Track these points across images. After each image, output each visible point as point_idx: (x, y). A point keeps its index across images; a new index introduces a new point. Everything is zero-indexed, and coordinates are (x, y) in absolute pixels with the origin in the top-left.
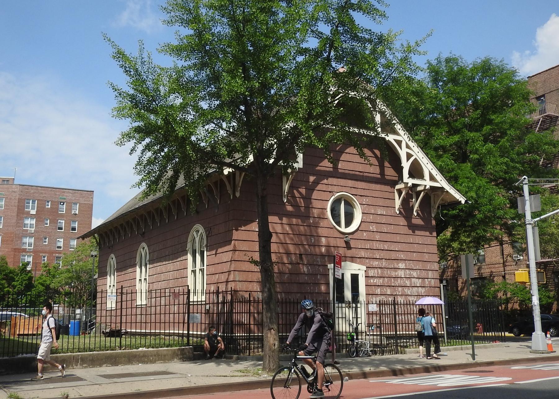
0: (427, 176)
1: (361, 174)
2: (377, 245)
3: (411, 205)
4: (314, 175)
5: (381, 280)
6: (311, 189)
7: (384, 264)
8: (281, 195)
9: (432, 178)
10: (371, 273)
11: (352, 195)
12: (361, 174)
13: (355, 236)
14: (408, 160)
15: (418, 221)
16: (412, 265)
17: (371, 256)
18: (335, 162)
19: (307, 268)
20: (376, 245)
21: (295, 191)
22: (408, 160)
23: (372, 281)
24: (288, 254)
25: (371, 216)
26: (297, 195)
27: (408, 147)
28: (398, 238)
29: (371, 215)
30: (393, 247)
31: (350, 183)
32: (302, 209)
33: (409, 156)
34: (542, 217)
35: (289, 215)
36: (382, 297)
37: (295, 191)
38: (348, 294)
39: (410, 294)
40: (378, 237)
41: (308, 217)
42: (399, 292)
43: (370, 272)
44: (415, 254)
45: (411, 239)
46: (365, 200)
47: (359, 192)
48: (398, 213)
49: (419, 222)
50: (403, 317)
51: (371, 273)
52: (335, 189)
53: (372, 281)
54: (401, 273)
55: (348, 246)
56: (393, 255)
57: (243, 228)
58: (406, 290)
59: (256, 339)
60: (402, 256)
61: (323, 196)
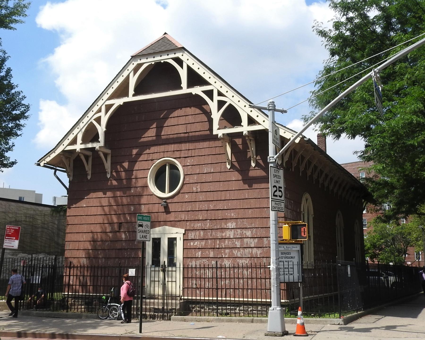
1: (187, 135)
3: (248, 157)
4: (136, 147)
5: (203, 243)
6: (133, 162)
7: (208, 225)
9: (251, 121)
10: (191, 235)
11: (175, 158)
12: (187, 135)
13: (175, 199)
14: (219, 109)
16: (246, 224)
17: (193, 218)
18: (160, 128)
19: (125, 235)
22: (219, 109)
23: (192, 244)
24: (111, 224)
25: (195, 177)
27: (220, 94)
28: (228, 195)
29: (196, 176)
30: (220, 205)
31: (172, 147)
32: (124, 181)
33: (221, 104)
35: (113, 189)
36: (204, 260)
37: (118, 167)
38: (164, 259)
39: (239, 255)
40: (202, 197)
41: (129, 188)
42: (225, 254)
43: (190, 235)
44: (250, 211)
46: (189, 161)
48: (229, 167)
51: (191, 235)
52: (155, 156)
54: (230, 234)
55: (167, 210)
57: (74, 206)
59: (80, 297)
60: (233, 215)
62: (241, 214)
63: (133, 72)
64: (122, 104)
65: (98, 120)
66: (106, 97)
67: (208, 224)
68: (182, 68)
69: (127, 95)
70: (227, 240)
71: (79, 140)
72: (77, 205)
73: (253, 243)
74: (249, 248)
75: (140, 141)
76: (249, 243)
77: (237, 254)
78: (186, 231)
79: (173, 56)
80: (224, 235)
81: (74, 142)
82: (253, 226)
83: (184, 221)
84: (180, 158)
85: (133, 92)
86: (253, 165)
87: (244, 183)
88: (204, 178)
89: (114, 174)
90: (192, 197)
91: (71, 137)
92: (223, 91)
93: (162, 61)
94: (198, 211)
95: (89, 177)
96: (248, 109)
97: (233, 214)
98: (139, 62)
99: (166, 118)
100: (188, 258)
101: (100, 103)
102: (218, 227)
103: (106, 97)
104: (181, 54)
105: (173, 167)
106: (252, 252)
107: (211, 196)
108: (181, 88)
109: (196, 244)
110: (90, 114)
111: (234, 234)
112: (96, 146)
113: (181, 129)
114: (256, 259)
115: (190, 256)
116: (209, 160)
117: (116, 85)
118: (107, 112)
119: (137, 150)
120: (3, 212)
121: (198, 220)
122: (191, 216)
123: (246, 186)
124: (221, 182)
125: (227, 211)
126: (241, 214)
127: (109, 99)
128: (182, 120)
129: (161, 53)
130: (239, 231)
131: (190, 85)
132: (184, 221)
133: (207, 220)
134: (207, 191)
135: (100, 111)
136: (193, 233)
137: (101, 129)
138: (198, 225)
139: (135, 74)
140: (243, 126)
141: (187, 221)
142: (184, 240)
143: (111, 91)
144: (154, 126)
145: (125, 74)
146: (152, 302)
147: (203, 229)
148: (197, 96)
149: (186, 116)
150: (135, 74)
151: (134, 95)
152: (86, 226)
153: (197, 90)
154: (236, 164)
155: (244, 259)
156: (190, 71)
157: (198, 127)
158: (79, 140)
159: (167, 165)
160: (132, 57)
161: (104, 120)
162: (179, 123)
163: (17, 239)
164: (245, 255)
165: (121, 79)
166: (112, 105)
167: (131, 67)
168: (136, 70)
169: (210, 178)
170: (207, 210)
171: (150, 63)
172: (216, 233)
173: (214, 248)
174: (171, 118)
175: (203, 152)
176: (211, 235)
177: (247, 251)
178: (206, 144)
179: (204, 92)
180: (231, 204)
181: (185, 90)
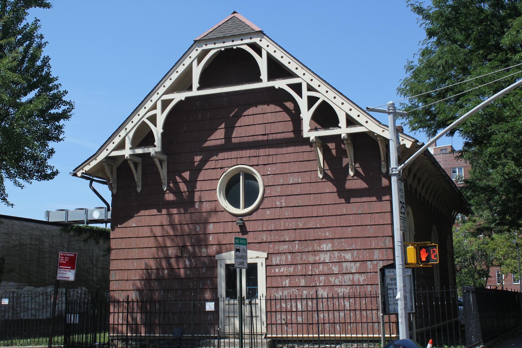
0: (343, 121)
2: (287, 224)
3: (344, 164)
5: (291, 269)
6: (196, 171)
7: (297, 247)
8: (161, 184)
9: (351, 122)
10: (276, 260)
12: (265, 138)
13: (254, 216)
14: (309, 108)
15: (354, 183)
16: (344, 244)
17: (277, 238)
19: (190, 261)
20: (282, 225)
21: (177, 177)
22: (309, 108)
23: (277, 270)
25: (279, 188)
26: (178, 179)
27: (310, 88)
28: (321, 211)
30: (311, 223)
31: (246, 153)
33: (312, 100)
34: (406, 162)
40: (287, 213)
42: (320, 282)
43: (274, 259)
44: (349, 229)
45: (345, 208)
46: (269, 170)
47: (261, 161)
48: (321, 176)
49: (360, 184)
50: (326, 315)
51: (276, 260)
52: (225, 163)
53: (277, 270)
56: (312, 234)
58: (332, 279)
61: (212, 174)
62: (339, 232)
63: (196, 60)
64: (183, 99)
65: (153, 119)
66: (162, 90)
67: (297, 246)
68: (261, 57)
69: (190, 88)
70: (321, 264)
71: (128, 145)
72: (124, 225)
73: (354, 268)
74: (350, 273)
75: (205, 145)
76: (349, 267)
77: (334, 281)
78: (270, 255)
79: (248, 41)
80: (317, 258)
81: (121, 146)
82: (354, 248)
83: (265, 242)
84: (258, 165)
85: (198, 85)
86: (351, 173)
87: (340, 197)
88: (290, 190)
89: (171, 185)
90: (277, 213)
91: (117, 140)
92: (315, 84)
93: (235, 48)
94: (284, 230)
95: (139, 190)
96: (347, 106)
97: (327, 234)
98: (205, 47)
99: (238, 116)
100: (273, 287)
101: (155, 98)
102: (310, 249)
103: (162, 90)
104: (259, 39)
105: (249, 177)
106: (353, 278)
107: (298, 212)
108: (261, 81)
109: (282, 270)
110: (142, 112)
111: (330, 257)
112: (152, 151)
113: (260, 130)
114: (358, 287)
115: (275, 285)
116: (295, 167)
117: (175, 76)
118: (163, 110)
119: (201, 157)
120: (5, 233)
121: (284, 241)
122: (274, 237)
123: (343, 201)
124: (312, 195)
125: (320, 230)
126: (339, 232)
127: (166, 93)
128: (259, 119)
129: (233, 38)
130: (336, 253)
131: (271, 77)
132: (265, 242)
133: (295, 241)
134: (295, 206)
135: (154, 107)
136: (278, 257)
137: (158, 131)
138: (285, 247)
139: (199, 62)
140: (340, 128)
141: (269, 242)
142: (266, 266)
143: (168, 83)
144: (223, 126)
145: (187, 62)
146: (232, 342)
147: (290, 253)
148: (281, 90)
149: (264, 114)
150: (199, 62)
151: (199, 89)
152: (137, 251)
153: (281, 84)
154: (329, 173)
155: (343, 287)
156: (271, 60)
157: (281, 127)
158: (128, 145)
159: (241, 174)
160: (195, 41)
161: (161, 119)
162: (256, 123)
163: (73, 268)
164: (345, 282)
165: (181, 69)
166: (171, 100)
167: (194, 54)
168: (200, 58)
169: (297, 190)
170: (295, 229)
171: (219, 49)
172: (307, 257)
173: (305, 275)
174: (245, 116)
175: (287, 158)
176: (301, 259)
177: (347, 277)
178: (291, 149)
179: (290, 86)
180: (324, 222)
181: (265, 83)
